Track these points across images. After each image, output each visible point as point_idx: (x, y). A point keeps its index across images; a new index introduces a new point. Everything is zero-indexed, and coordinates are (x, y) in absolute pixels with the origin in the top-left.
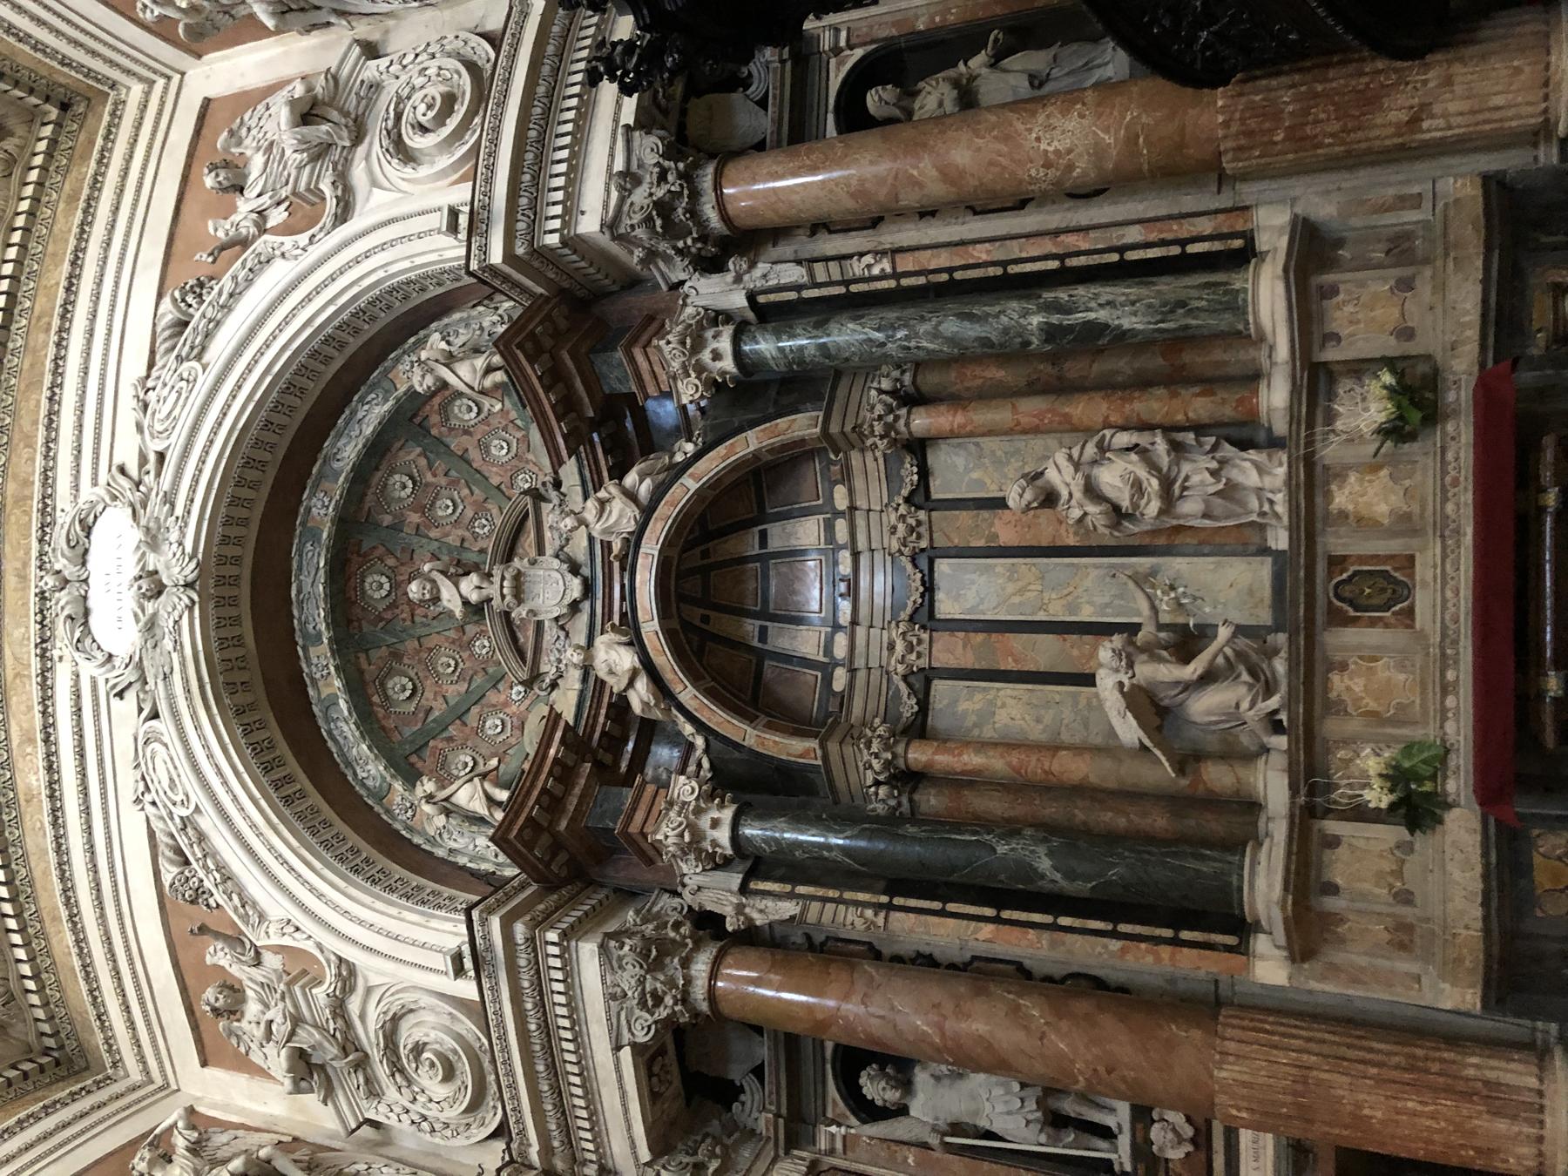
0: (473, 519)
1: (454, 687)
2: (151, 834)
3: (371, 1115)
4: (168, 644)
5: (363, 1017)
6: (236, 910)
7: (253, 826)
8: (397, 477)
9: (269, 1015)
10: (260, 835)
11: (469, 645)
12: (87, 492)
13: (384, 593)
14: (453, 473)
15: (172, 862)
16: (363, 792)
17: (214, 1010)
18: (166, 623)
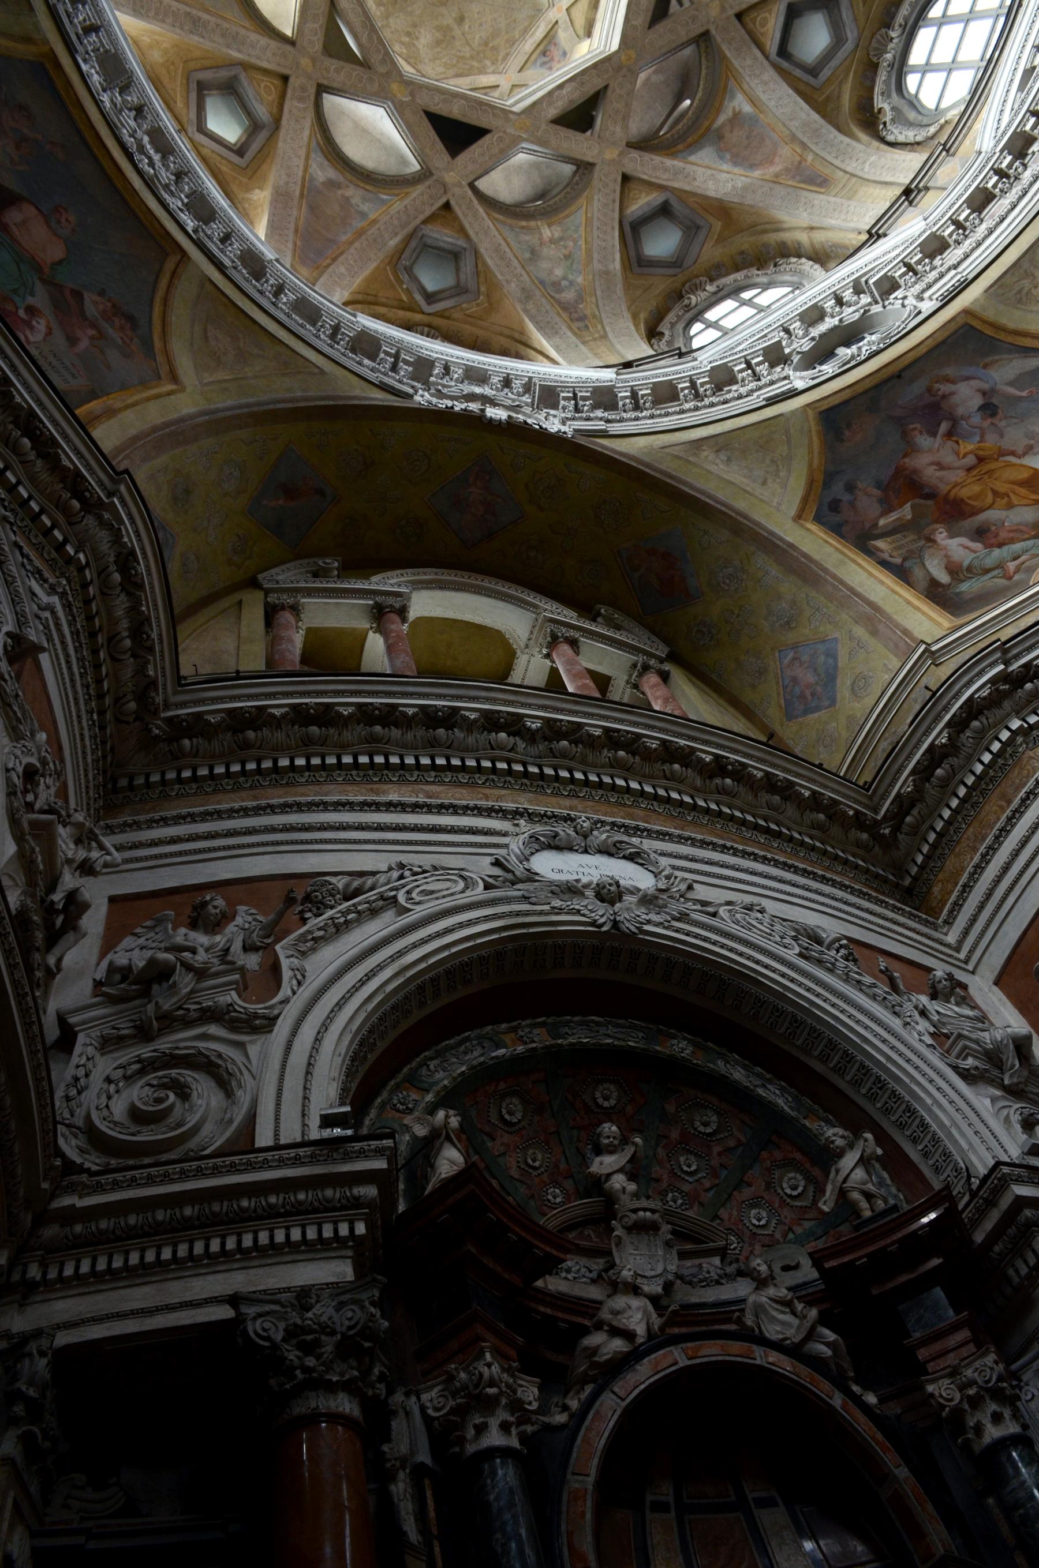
0: (681, 1192)
1: (514, 1164)
2: (373, 874)
3: (81, 1038)
4: (557, 903)
5: (205, 1037)
6: (309, 932)
7: (401, 954)
8: (714, 1118)
9: (201, 951)
10: (393, 958)
11: (557, 1184)
12: (664, 861)
13: (600, 1101)
14: (724, 1173)
15: (347, 885)
16: (414, 1064)
17: (204, 904)
18: (576, 904)
